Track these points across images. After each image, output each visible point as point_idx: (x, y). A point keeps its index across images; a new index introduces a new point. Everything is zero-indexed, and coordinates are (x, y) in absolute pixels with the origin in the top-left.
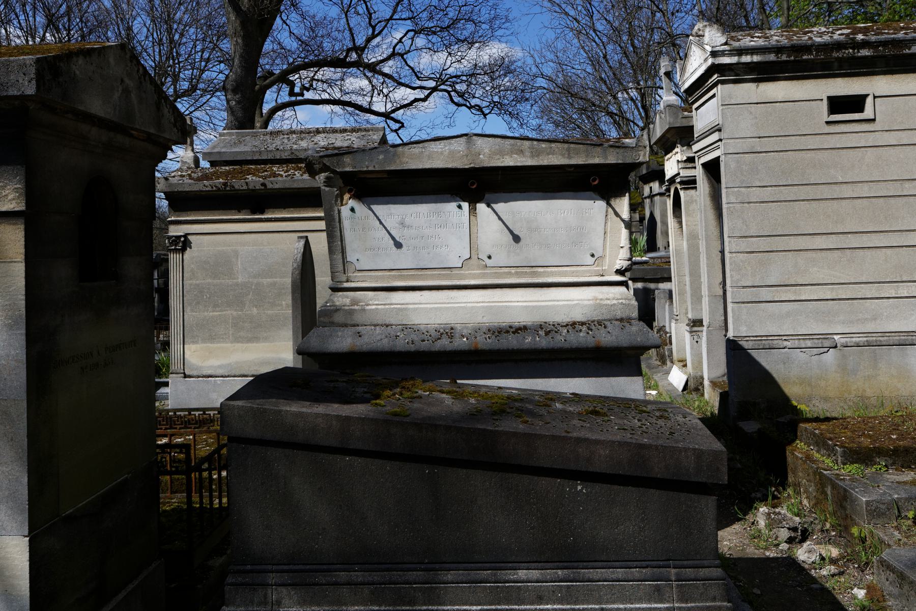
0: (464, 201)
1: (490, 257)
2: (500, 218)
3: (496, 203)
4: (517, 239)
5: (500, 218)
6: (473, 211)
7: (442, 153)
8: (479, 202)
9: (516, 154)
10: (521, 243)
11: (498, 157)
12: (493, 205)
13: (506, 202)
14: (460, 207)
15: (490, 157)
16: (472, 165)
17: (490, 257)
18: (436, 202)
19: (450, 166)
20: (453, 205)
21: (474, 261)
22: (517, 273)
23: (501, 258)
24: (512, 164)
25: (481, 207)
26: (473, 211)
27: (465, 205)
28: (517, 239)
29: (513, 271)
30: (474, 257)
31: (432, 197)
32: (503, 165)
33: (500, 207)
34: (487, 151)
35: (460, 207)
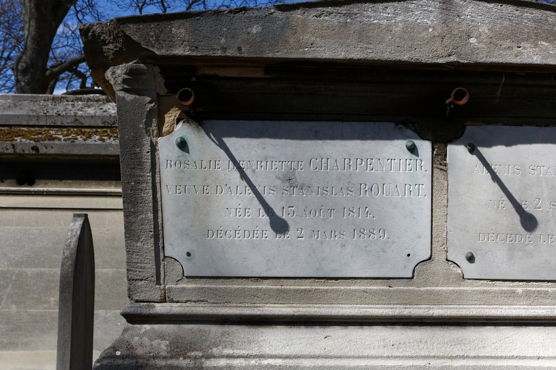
0: (423, 138)
1: (471, 259)
2: (495, 178)
3: (489, 145)
4: (529, 222)
5: (495, 178)
6: (439, 160)
7: (388, 29)
8: (454, 139)
9: (546, 39)
10: (537, 232)
11: (508, 43)
12: (484, 151)
13: (509, 143)
14: (413, 150)
15: (492, 43)
16: (453, 59)
17: (471, 259)
18: (363, 137)
19: (405, 57)
20: (397, 148)
21: (438, 265)
22: (527, 294)
23: (497, 260)
24: (536, 60)
25: (457, 152)
26: (439, 160)
27: (425, 147)
28: (529, 222)
29: (520, 288)
30: (440, 257)
31: (357, 126)
32: (518, 60)
33: (496, 154)
34: (484, 29)
35: (413, 150)
